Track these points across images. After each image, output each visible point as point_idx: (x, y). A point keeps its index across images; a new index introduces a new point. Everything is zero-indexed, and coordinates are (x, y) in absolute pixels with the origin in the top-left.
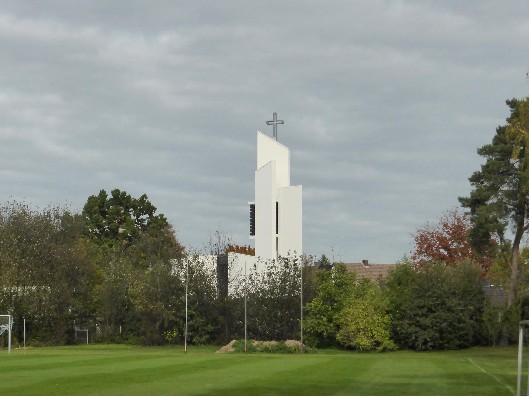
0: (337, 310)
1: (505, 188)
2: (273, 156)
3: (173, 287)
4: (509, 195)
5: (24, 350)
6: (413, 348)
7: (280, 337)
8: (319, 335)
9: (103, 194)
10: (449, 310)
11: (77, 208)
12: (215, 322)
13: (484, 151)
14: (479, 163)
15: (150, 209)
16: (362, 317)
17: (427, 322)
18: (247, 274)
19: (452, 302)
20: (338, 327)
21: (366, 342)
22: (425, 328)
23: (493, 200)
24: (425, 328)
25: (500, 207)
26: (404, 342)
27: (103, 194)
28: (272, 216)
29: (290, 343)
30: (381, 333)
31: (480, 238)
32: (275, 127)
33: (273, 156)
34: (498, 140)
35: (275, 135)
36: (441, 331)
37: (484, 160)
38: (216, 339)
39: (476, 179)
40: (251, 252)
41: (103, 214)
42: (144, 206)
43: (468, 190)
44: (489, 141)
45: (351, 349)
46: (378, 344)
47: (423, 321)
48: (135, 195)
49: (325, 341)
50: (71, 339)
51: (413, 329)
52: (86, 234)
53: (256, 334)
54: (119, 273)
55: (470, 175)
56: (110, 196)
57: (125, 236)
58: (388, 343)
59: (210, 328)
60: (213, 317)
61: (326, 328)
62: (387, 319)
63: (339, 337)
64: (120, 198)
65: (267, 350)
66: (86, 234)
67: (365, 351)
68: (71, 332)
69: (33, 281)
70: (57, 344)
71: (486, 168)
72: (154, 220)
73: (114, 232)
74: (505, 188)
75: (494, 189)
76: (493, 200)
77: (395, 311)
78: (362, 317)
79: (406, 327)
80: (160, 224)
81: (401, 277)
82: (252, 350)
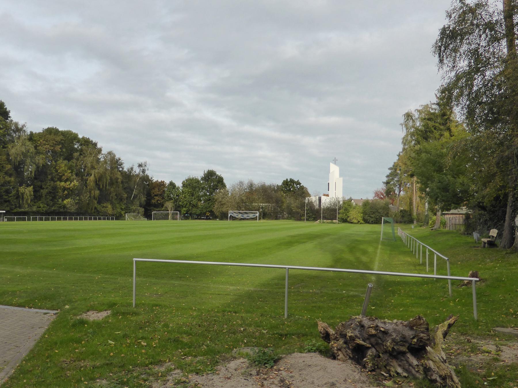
0: (348, 212)
1: (396, 179)
2: (335, 169)
3: (303, 205)
4: (397, 181)
5: (262, 221)
6: (369, 223)
7: (332, 219)
8: (343, 219)
9: (287, 180)
10: (379, 213)
11: (280, 183)
12: (315, 215)
13: (390, 169)
14: (388, 172)
15: (300, 184)
16: (355, 215)
17: (373, 216)
18: (326, 201)
19: (380, 211)
20: (348, 217)
21: (356, 221)
22: (372, 217)
23: (392, 182)
24: (372, 217)
25: (394, 185)
26: (366, 221)
27: (287, 180)
28: (332, 187)
29: (334, 221)
30: (360, 219)
31: (389, 192)
32: (335, 161)
33: (335, 169)
34: (394, 166)
35: (335, 163)
36: (377, 219)
37: (390, 171)
38: (315, 219)
39: (387, 176)
40: (328, 195)
41: (287, 185)
42: (298, 183)
43: (385, 179)
44: (391, 166)
45: (352, 223)
46: (359, 222)
47: (371, 216)
48: (296, 180)
49: (345, 221)
50: (277, 218)
51: (369, 218)
52: (282, 190)
53: (325, 218)
54: (289, 201)
55: (174, 182)
56: (289, 180)
57: (293, 191)
58: (362, 221)
59: (314, 216)
60: (314, 214)
61: (345, 217)
62: (362, 215)
63: (348, 220)
64: (292, 181)
65: (328, 223)
66: (282, 190)
67: (355, 223)
68: (277, 216)
69: (267, 202)
70: (273, 219)
71: (390, 173)
72: (301, 187)
73: (290, 189)
74: (396, 179)
75: (393, 179)
76: (392, 182)
77: (364, 213)
78: (355, 215)
79: (366, 217)
80: (302, 188)
81: (366, 203)
82: (324, 223)
